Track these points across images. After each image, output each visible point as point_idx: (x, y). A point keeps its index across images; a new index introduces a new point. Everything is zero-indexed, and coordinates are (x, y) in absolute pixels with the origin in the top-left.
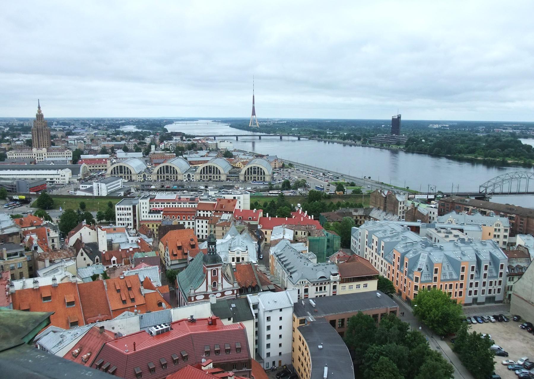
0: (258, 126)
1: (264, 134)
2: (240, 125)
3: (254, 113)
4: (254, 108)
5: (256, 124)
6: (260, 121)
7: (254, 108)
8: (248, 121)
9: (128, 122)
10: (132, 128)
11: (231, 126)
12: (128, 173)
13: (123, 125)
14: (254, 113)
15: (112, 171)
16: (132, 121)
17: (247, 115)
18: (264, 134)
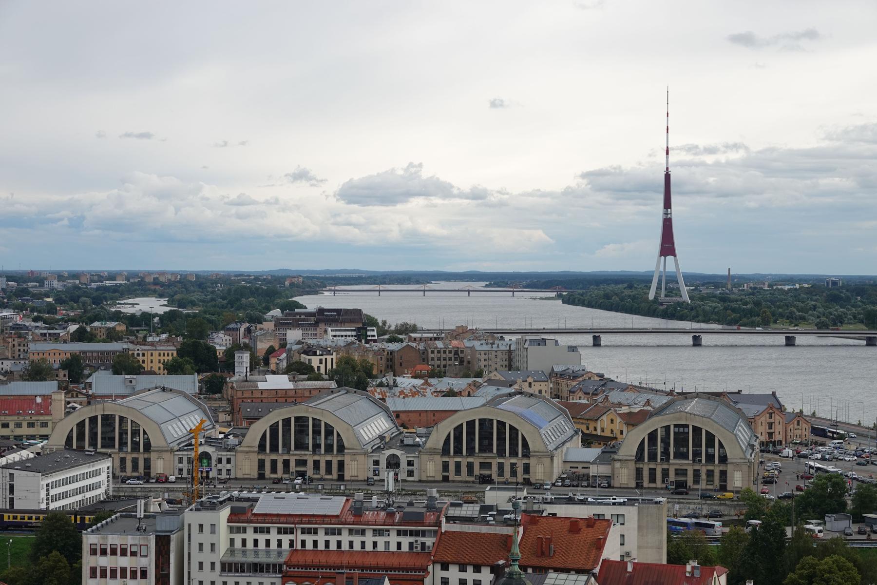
0: (686, 298)
2: (607, 296)
3: (668, 247)
4: (667, 225)
6: (695, 281)
7: (667, 225)
8: (645, 280)
9: (141, 285)
10: (155, 305)
11: (568, 301)
12: (135, 447)
13: (120, 292)
14: (668, 247)
15: (69, 439)
16: (156, 282)
17: (638, 256)
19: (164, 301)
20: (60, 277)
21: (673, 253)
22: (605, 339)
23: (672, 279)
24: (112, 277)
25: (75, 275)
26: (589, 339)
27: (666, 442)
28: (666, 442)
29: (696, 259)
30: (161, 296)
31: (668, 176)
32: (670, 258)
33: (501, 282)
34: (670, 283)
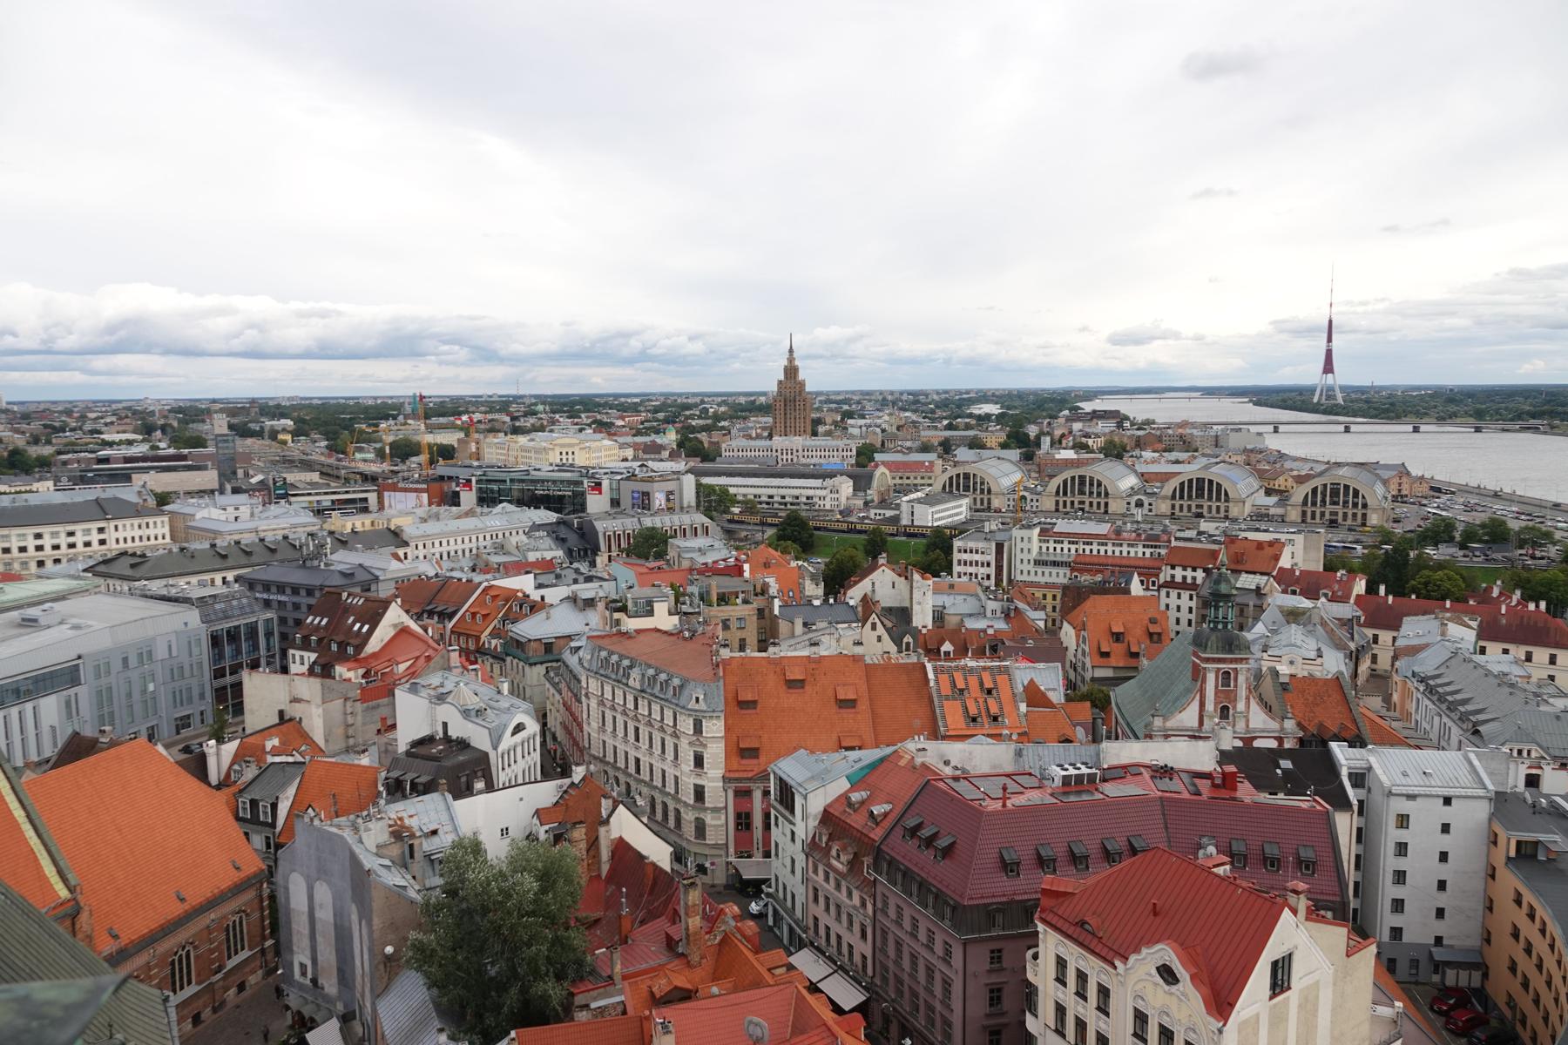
2: (1284, 401)
3: (1328, 368)
4: (1329, 354)
5: (1334, 397)
7: (1329, 354)
8: (1312, 390)
9: (984, 397)
10: (994, 409)
11: (1256, 404)
12: (982, 491)
14: (1328, 368)
17: (1306, 373)
20: (938, 393)
22: (1282, 428)
23: (1330, 389)
24: (968, 392)
25: (946, 392)
26: (1271, 428)
27: (1190, 487)
28: (1190, 487)
29: (1348, 375)
31: (1330, 322)
33: (1210, 392)
34: (1329, 392)
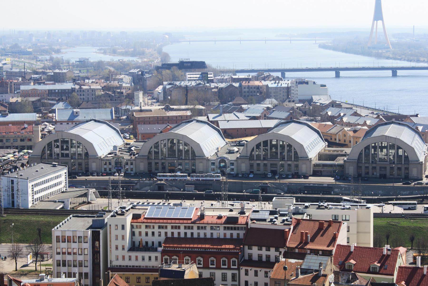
1: (276, 195)
3: (378, 15)
14: (378, 15)
18: (276, 195)
19: (95, 49)
21: (381, 19)
22: (342, 73)
26: (333, 73)
30: (93, 45)
32: (380, 22)
